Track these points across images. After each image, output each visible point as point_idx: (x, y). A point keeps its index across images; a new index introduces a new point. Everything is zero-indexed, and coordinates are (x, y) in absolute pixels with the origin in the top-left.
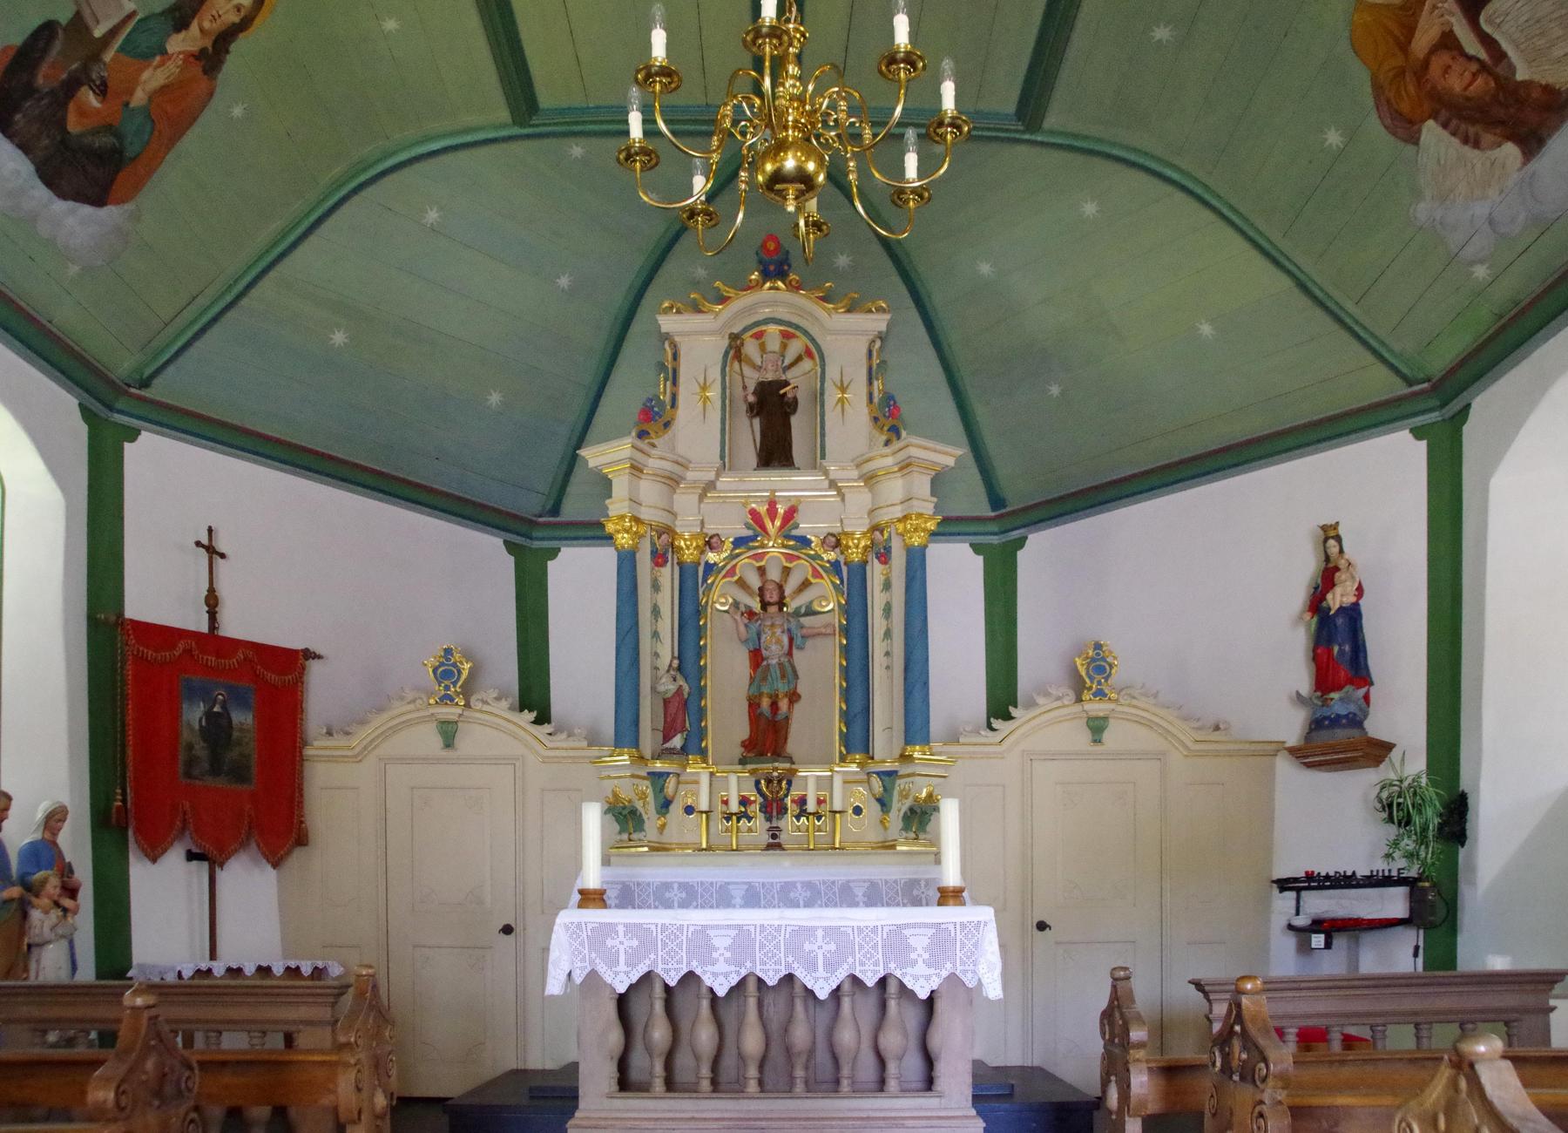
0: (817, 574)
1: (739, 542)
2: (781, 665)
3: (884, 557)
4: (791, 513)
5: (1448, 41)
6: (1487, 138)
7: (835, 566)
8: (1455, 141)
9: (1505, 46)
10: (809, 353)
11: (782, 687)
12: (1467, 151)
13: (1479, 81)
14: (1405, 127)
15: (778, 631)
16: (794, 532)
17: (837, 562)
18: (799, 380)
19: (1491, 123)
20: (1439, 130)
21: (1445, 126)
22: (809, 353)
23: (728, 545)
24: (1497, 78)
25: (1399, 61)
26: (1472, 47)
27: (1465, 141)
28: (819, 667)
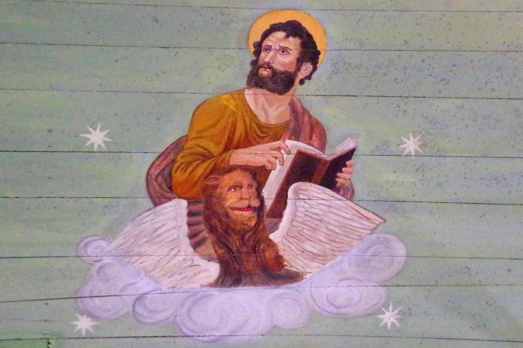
5: (259, 175)
6: (209, 248)
8: (185, 229)
9: (287, 213)
12: (186, 242)
13: (247, 214)
14: (162, 185)
19: (222, 241)
20: (185, 212)
21: (190, 214)
24: (258, 224)
25: (215, 149)
26: (269, 192)
27: (192, 236)
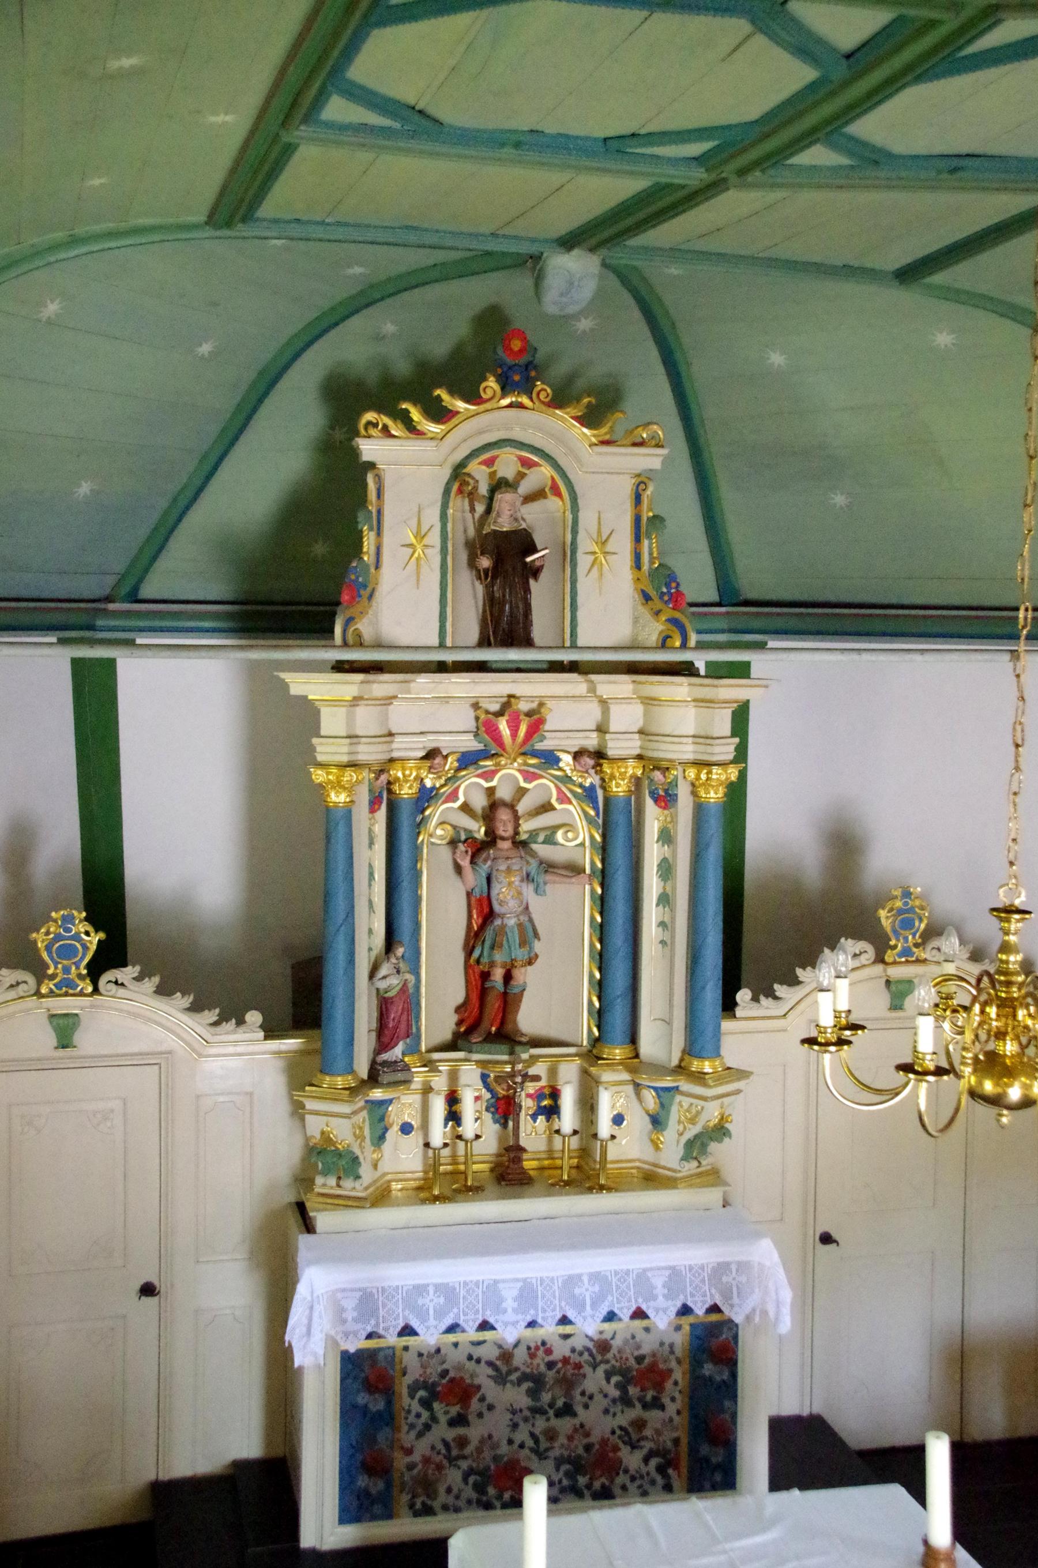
0: (563, 799)
1: (468, 760)
2: (520, 926)
3: (666, 799)
4: (536, 726)
7: (589, 794)
10: (557, 493)
11: (520, 954)
15: (515, 879)
16: (539, 746)
17: (593, 786)
18: (540, 518)
22: (557, 493)
23: (452, 762)
28: (563, 920)
